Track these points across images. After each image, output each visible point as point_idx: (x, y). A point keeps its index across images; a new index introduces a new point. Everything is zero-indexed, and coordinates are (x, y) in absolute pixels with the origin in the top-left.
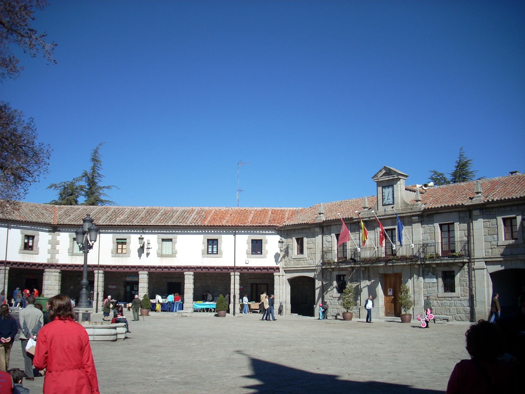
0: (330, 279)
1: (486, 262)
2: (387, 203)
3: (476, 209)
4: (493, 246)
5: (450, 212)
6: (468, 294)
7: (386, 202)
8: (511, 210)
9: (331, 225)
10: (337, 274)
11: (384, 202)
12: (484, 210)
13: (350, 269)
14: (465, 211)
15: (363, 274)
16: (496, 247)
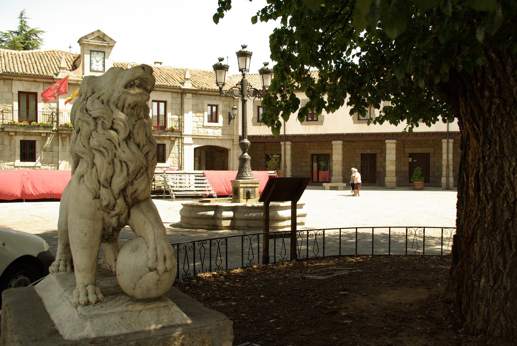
0: (10, 145)
1: (193, 138)
2: (96, 70)
3: (189, 93)
4: (199, 126)
5: (164, 91)
6: (177, 165)
7: (94, 67)
8: (215, 99)
9: (12, 80)
10: (22, 139)
11: (92, 67)
12: (194, 95)
13: (45, 135)
14: (178, 93)
15: (62, 141)
16: (201, 127)
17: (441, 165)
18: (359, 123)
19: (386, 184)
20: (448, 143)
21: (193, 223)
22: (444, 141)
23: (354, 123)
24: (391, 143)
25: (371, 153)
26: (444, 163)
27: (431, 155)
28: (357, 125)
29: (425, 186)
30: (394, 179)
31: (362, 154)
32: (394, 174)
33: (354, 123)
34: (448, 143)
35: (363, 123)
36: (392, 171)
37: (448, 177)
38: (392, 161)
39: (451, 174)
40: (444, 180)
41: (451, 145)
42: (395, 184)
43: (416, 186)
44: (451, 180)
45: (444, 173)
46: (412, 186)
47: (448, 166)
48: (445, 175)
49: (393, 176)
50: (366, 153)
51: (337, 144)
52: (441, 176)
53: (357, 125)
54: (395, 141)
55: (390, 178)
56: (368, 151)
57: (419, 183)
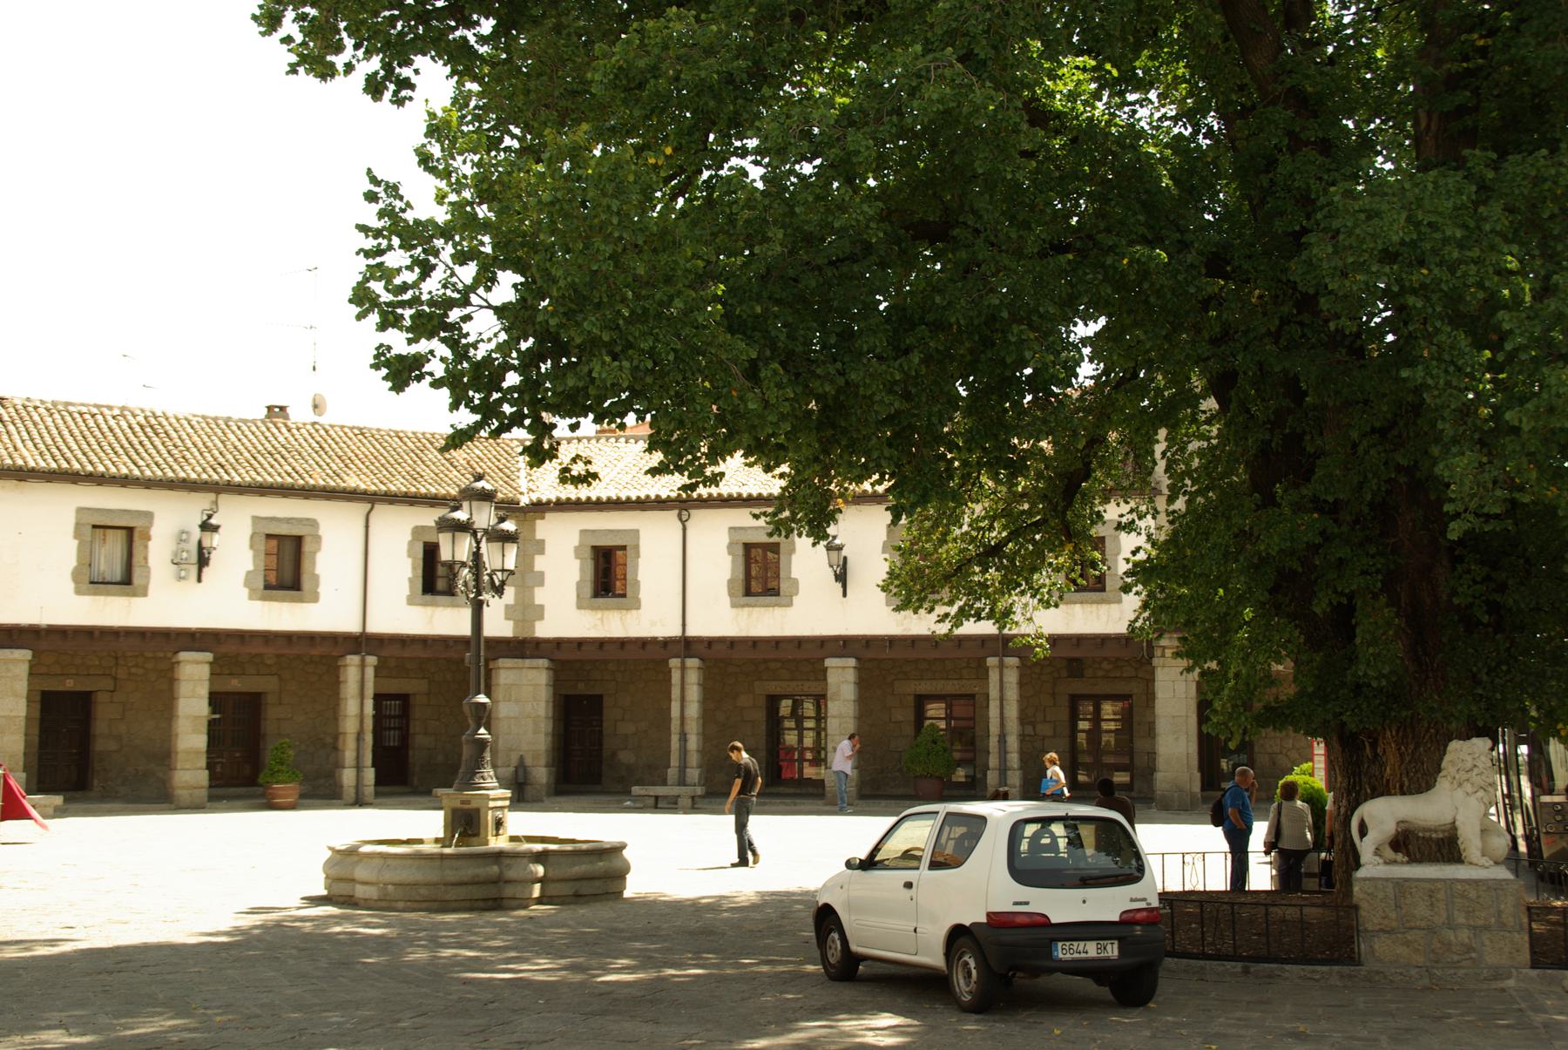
17: (337, 736)
18: (95, 594)
19: (179, 792)
20: (363, 666)
21: (447, 897)
22: (353, 660)
23: (78, 592)
24: (198, 663)
25: (79, 688)
26: (350, 726)
27: (270, 699)
28: (87, 600)
29: (303, 796)
30: (203, 777)
31: (43, 693)
32: (203, 762)
33: (78, 592)
34: (363, 666)
35: (108, 594)
36: (197, 752)
37: (359, 768)
38: (197, 718)
39: (368, 758)
40: (348, 777)
41: (370, 672)
42: (204, 793)
43: (281, 797)
44: (370, 775)
45: (349, 755)
46: (263, 795)
47: (359, 737)
48: (353, 763)
49: (200, 769)
50: (60, 688)
51: (18, 661)
52: (339, 765)
53: (87, 599)
54: (209, 656)
55: (191, 771)
56: (69, 685)
57: (286, 789)
